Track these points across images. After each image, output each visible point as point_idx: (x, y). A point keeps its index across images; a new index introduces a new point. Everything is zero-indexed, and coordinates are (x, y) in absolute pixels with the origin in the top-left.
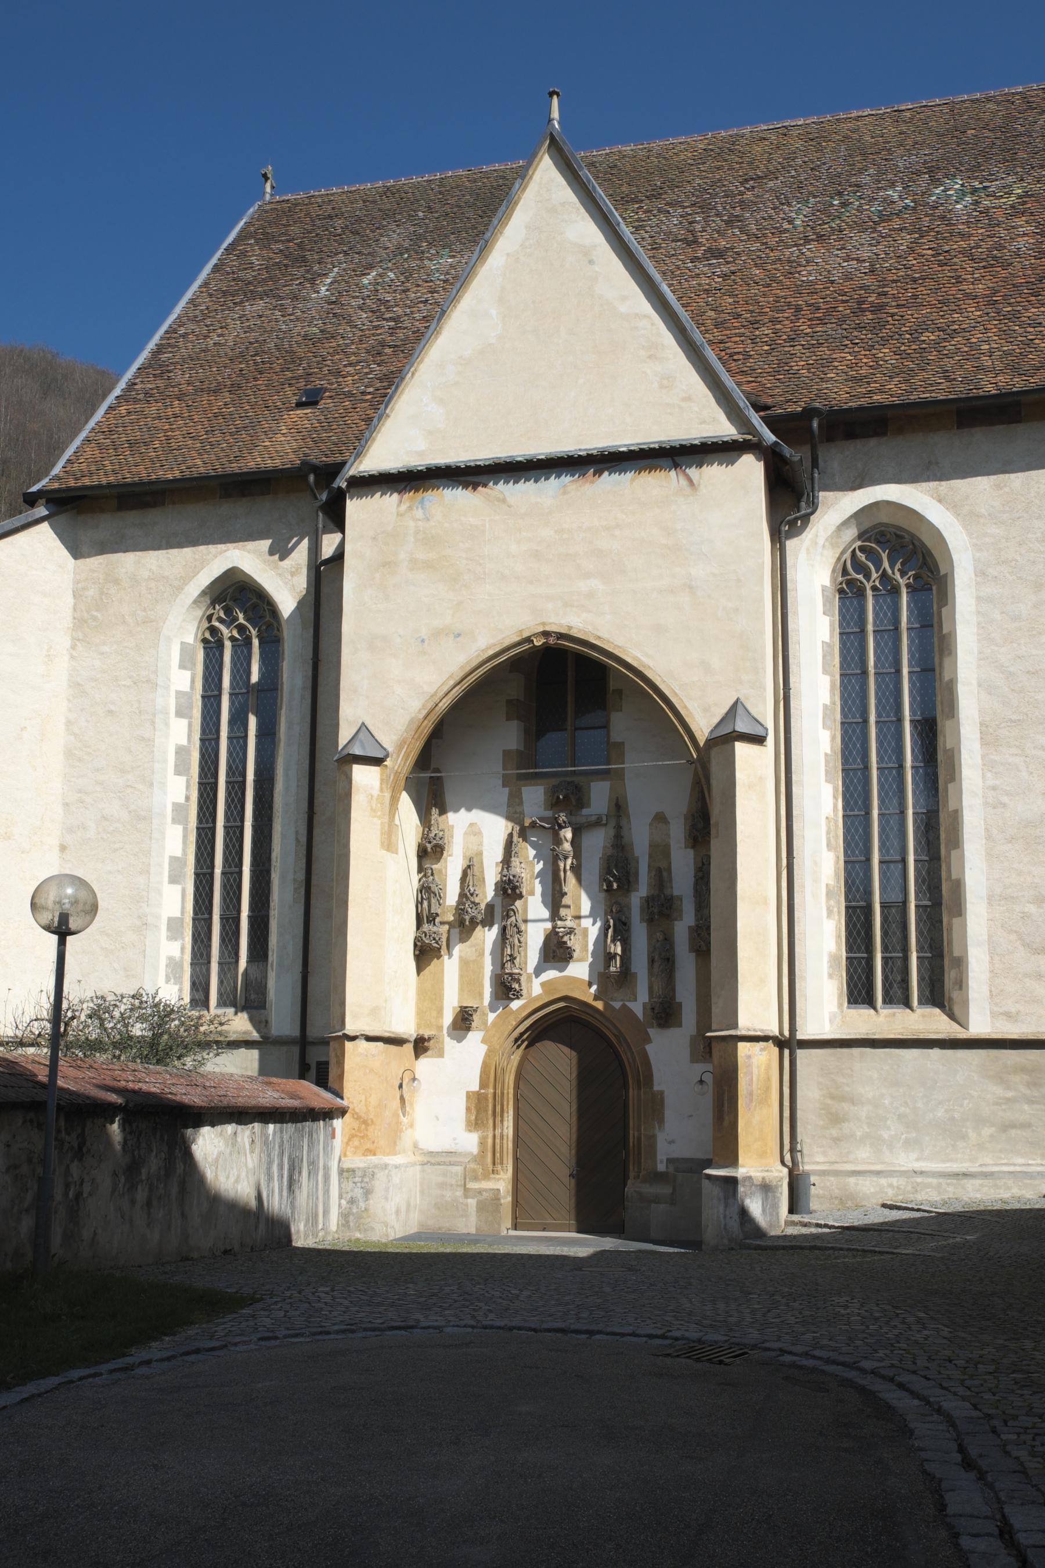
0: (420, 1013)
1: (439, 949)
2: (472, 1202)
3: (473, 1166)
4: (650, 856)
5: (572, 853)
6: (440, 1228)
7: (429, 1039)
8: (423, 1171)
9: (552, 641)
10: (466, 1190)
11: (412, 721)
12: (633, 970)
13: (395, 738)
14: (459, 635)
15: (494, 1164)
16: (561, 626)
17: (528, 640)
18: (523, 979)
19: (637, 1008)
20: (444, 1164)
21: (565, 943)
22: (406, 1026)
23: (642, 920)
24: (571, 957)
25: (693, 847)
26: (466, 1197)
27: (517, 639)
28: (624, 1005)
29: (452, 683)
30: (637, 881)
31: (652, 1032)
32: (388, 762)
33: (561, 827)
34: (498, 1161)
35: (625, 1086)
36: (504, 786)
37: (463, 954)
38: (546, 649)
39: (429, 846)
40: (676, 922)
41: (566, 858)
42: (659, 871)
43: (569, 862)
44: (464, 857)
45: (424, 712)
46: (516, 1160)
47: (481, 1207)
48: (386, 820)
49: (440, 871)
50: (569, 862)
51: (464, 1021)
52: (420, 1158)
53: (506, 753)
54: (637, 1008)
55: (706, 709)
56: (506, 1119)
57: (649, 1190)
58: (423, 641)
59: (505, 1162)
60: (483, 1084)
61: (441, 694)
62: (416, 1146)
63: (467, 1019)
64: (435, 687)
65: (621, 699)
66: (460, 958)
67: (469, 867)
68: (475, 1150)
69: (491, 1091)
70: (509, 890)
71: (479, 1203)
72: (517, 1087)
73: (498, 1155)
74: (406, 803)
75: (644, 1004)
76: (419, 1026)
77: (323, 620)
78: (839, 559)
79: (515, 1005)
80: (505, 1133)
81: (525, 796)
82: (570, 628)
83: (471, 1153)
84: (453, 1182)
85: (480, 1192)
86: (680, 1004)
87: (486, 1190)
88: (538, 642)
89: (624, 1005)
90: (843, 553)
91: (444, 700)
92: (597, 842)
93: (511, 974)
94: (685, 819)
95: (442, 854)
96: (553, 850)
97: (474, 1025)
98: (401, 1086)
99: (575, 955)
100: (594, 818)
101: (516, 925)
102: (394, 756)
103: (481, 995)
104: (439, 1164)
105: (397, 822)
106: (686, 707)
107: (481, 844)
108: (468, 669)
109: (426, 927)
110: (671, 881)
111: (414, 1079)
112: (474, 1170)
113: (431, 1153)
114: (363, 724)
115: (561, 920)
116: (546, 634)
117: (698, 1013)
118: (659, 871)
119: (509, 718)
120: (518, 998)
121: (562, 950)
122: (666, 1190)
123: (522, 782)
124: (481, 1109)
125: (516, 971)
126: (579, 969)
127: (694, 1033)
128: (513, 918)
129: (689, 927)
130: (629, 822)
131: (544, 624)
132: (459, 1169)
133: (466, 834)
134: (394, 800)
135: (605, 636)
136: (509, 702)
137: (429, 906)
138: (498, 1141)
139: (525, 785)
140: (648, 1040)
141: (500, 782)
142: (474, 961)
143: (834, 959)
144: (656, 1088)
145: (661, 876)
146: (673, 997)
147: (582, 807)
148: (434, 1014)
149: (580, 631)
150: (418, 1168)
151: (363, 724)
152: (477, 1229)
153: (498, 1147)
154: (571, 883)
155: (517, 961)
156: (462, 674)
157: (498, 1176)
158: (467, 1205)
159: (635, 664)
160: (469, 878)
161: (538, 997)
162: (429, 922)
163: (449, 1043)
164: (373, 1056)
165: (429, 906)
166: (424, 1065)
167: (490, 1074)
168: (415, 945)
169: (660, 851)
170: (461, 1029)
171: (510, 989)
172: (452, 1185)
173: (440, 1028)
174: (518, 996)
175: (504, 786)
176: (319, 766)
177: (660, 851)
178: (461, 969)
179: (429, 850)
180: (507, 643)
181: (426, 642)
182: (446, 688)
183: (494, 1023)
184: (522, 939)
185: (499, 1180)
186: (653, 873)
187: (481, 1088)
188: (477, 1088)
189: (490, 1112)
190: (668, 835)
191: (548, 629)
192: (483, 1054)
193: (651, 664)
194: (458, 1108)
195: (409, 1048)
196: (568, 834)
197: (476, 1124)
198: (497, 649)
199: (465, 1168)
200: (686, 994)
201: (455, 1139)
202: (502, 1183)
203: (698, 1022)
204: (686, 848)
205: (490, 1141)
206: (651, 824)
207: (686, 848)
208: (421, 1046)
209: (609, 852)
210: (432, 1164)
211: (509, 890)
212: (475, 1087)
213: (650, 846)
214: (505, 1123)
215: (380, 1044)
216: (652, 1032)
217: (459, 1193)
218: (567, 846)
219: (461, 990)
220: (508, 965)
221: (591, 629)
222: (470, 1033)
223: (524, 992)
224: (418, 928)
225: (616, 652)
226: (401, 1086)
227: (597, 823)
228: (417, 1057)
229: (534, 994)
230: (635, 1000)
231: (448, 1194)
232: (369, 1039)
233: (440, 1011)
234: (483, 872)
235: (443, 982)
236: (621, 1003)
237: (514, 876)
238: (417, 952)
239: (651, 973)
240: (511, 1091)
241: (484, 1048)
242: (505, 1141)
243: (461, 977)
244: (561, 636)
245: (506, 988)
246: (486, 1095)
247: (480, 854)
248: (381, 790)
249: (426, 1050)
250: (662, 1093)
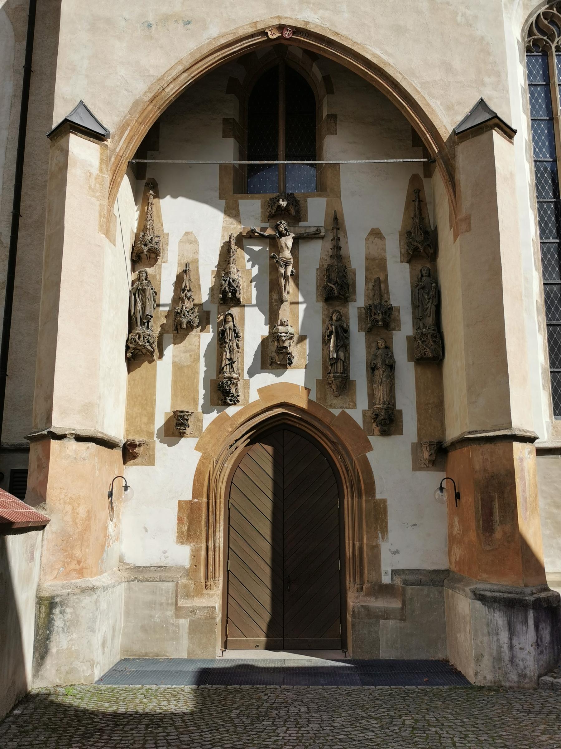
0: (130, 419)
1: (152, 353)
2: (184, 622)
3: (184, 581)
4: (367, 269)
5: (292, 260)
6: (146, 654)
7: (140, 445)
8: (129, 589)
9: (287, 34)
10: (177, 608)
11: (136, 103)
12: (353, 376)
13: (117, 119)
14: (189, 23)
15: (207, 578)
16: (297, 20)
17: (263, 33)
18: (240, 385)
19: (357, 415)
20: (154, 580)
21: (286, 348)
22: (117, 431)
23: (360, 329)
24: (290, 364)
25: (409, 262)
26: (177, 617)
27: (251, 30)
28: (343, 413)
29: (180, 68)
30: (355, 291)
31: (374, 440)
32: (108, 142)
33: (282, 235)
34: (210, 574)
35: (340, 495)
36: (220, 198)
37: (177, 360)
38: (279, 46)
39: (145, 249)
40: (394, 332)
41: (286, 265)
42: (378, 281)
43: (290, 269)
44: (180, 264)
45: (150, 95)
46: (227, 572)
47: (194, 628)
48: (105, 202)
49: (154, 277)
50: (290, 269)
51: (177, 427)
52: (126, 574)
53: (223, 168)
54: (357, 415)
55: (449, 108)
56: (218, 529)
57: (378, 603)
58: (150, 26)
59: (217, 575)
60: (196, 493)
61: (169, 78)
62: (121, 560)
63: (182, 424)
64: (163, 71)
65: (336, 124)
66: (174, 364)
67: (185, 271)
68: (187, 564)
69: (205, 500)
70: (227, 296)
71: (192, 623)
72: (228, 495)
73: (211, 568)
74: (125, 186)
75: (364, 412)
76: (127, 431)
77: (36, 35)
78: (527, 21)
79: (231, 411)
80: (217, 545)
81: (242, 209)
82: (307, 23)
83: (183, 567)
84: (163, 600)
85: (193, 611)
86: (400, 412)
87: (199, 608)
88: (273, 35)
89: (343, 413)
90: (530, 16)
91: (172, 86)
92: (315, 254)
93: (230, 379)
94: (400, 236)
95: (156, 260)
96: (272, 258)
97: (188, 430)
98: (110, 494)
99: (295, 361)
100: (313, 230)
101: (234, 330)
102: (116, 137)
103: (195, 401)
104: (148, 581)
105: (115, 211)
106: (428, 105)
107: (197, 252)
108: (198, 56)
109: (139, 329)
110: (388, 293)
111: (126, 488)
112: (185, 586)
113: (138, 569)
114: (81, 102)
115: (282, 325)
116: (281, 28)
117: (419, 420)
118: (378, 281)
119: (225, 136)
120: (235, 404)
121: (281, 356)
122: (396, 604)
123: (239, 195)
124: (194, 519)
125: (235, 376)
126: (296, 376)
127: (416, 441)
128: (231, 324)
129: (408, 337)
130: (346, 236)
131: (279, 18)
132: (170, 586)
133: (181, 241)
134: (114, 184)
135: (344, 33)
136: (226, 121)
137: (144, 308)
138: (211, 553)
139: (241, 198)
140: (368, 447)
141: (217, 194)
142: (188, 367)
143: (544, 369)
144: (378, 497)
145: (379, 287)
146: (394, 405)
147: (299, 220)
148: (145, 419)
149: (317, 26)
150: (124, 585)
151: (81, 102)
152: (189, 654)
153: (211, 560)
154: (290, 290)
155: (235, 365)
156: (191, 60)
157: (211, 592)
158: (178, 626)
159: (375, 61)
160: (186, 282)
161: (255, 403)
162: (142, 324)
163: (160, 448)
164: (84, 459)
165: (144, 308)
166: (133, 473)
167: (203, 482)
168: (127, 348)
169: (377, 265)
170: (173, 435)
171: (227, 393)
172: (161, 604)
173: (151, 434)
174: (235, 402)
175: (220, 198)
176: (26, 170)
177: (377, 265)
178: (174, 374)
179: (145, 251)
180: (241, 33)
181: (154, 27)
182: (174, 73)
183: (209, 430)
184: (240, 345)
185: (212, 596)
186: (371, 285)
187: (194, 497)
188: (190, 498)
189: (203, 523)
190: (384, 250)
191: (283, 22)
192: (197, 461)
193: (391, 61)
194: (170, 518)
195: (118, 453)
196: (288, 241)
197: (189, 535)
198: (230, 38)
199: (177, 584)
200: (407, 402)
201: (165, 552)
202: (214, 599)
203: (419, 430)
204: (401, 262)
205: (203, 553)
206: (367, 239)
207: (401, 262)
208: (129, 452)
209: (329, 261)
210: (140, 581)
211: (227, 296)
212: (188, 496)
213: (367, 259)
214: (217, 534)
215: (92, 445)
216: (374, 440)
217: (170, 613)
218: (287, 254)
219: (175, 395)
220: (226, 369)
221: (328, 25)
222: (183, 439)
223: (241, 398)
224: (130, 331)
225: (355, 48)
226: (110, 494)
227: (315, 236)
228: (125, 462)
229: (251, 401)
230: (355, 407)
231: (157, 615)
232: (79, 438)
233: (151, 417)
234: (198, 279)
235: (155, 387)
236: (340, 410)
237: (234, 281)
238: (129, 355)
239: (371, 380)
240: (222, 500)
241: (198, 455)
242: (217, 553)
243: (175, 382)
244: (297, 30)
245: (222, 393)
246: (200, 504)
247: (196, 261)
248: (101, 170)
249: (134, 456)
250: (384, 501)
